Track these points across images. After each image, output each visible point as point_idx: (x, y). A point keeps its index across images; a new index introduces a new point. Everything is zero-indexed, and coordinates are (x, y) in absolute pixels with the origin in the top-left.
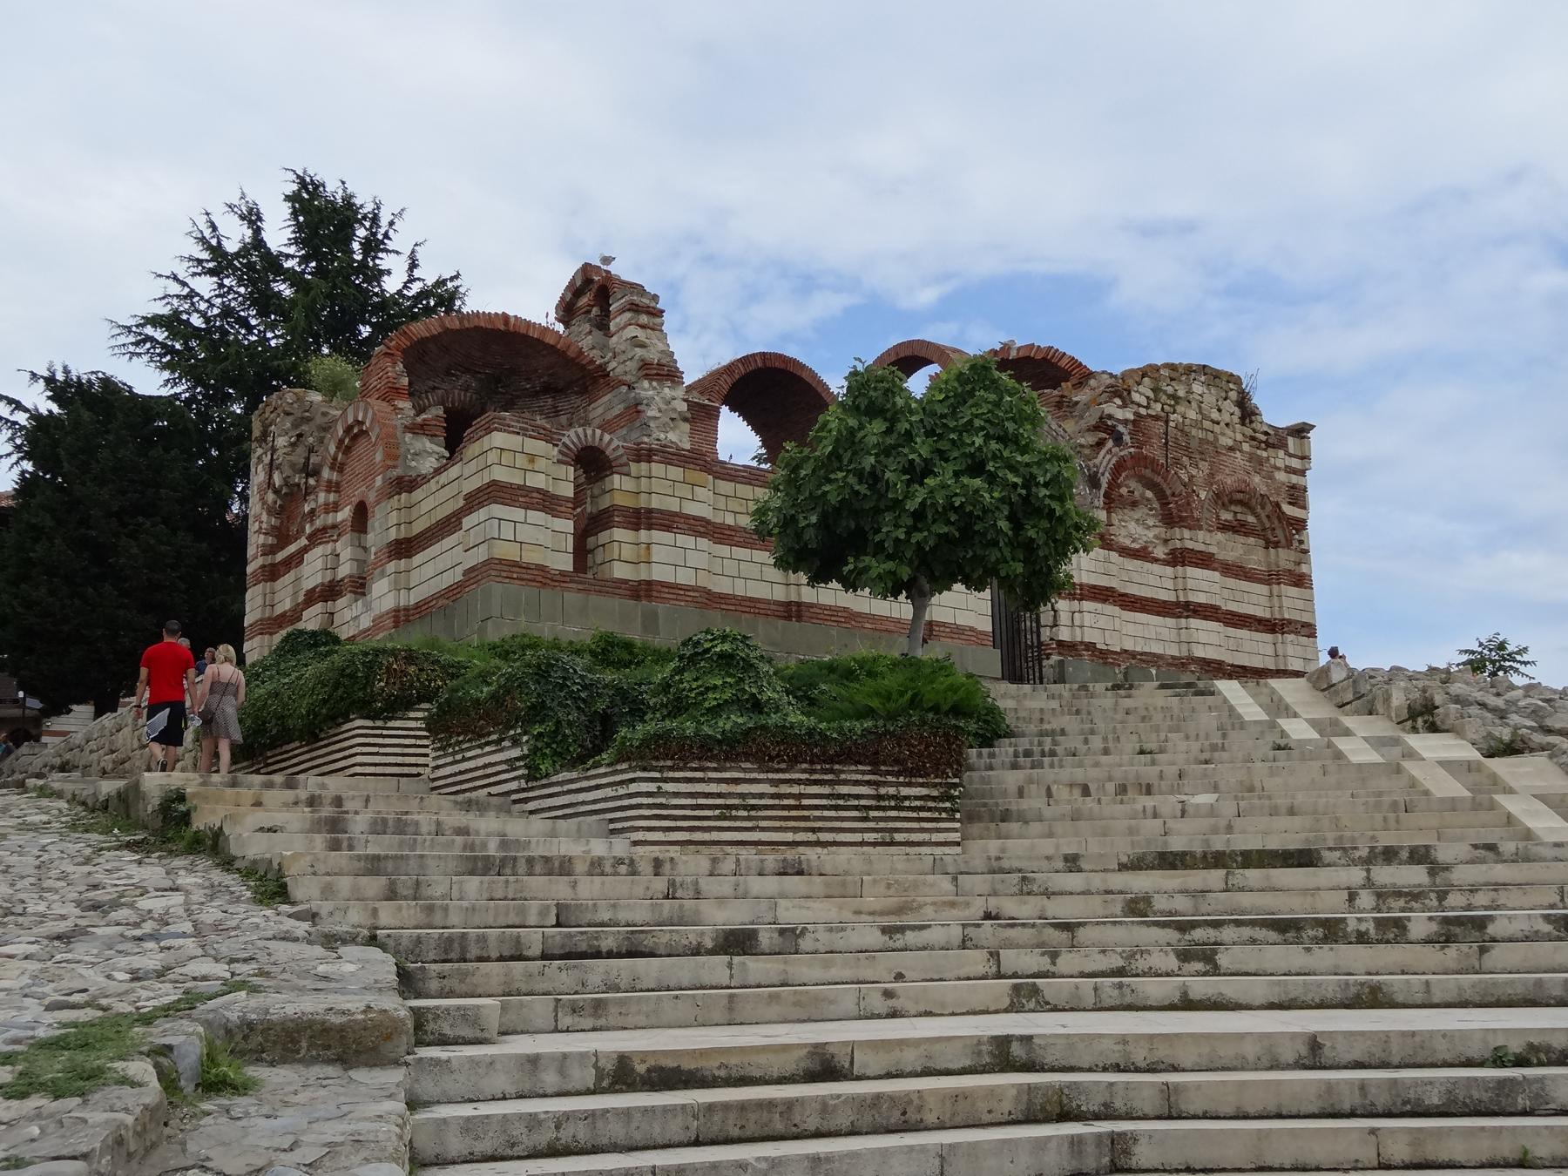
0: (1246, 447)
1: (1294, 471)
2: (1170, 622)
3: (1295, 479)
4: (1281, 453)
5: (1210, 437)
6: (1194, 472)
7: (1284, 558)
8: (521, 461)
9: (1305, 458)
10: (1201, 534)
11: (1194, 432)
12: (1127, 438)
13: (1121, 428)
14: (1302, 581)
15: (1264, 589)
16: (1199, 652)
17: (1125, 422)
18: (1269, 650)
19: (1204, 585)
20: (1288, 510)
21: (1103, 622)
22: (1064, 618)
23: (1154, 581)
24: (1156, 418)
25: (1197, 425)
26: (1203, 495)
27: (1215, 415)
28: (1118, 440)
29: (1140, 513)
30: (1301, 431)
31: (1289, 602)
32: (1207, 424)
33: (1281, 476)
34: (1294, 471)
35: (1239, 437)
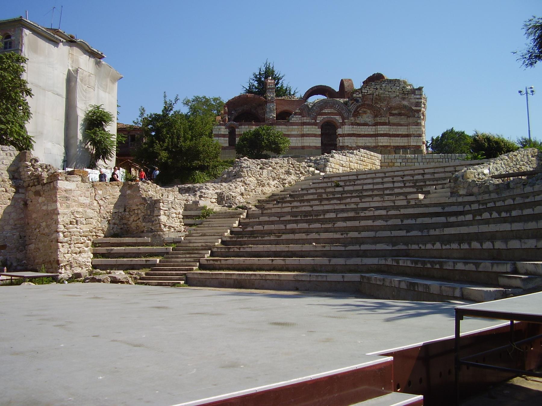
0: (400, 96)
1: (418, 99)
2: (373, 138)
3: (417, 100)
4: (413, 95)
5: (388, 96)
6: (382, 104)
7: (411, 120)
8: (217, 130)
9: (421, 95)
10: (383, 118)
11: (382, 96)
12: (360, 100)
13: (358, 99)
14: (418, 124)
15: (406, 127)
16: (380, 144)
17: (360, 97)
18: (406, 141)
19: (382, 129)
20: (414, 108)
21: (351, 141)
22: (341, 141)
23: (370, 130)
24: (370, 94)
25: (384, 94)
26: (384, 109)
27: (390, 90)
28: (357, 101)
29: (368, 114)
30: (420, 89)
31: (413, 130)
32: (387, 93)
33: (413, 101)
34: (418, 99)
35: (398, 94)
